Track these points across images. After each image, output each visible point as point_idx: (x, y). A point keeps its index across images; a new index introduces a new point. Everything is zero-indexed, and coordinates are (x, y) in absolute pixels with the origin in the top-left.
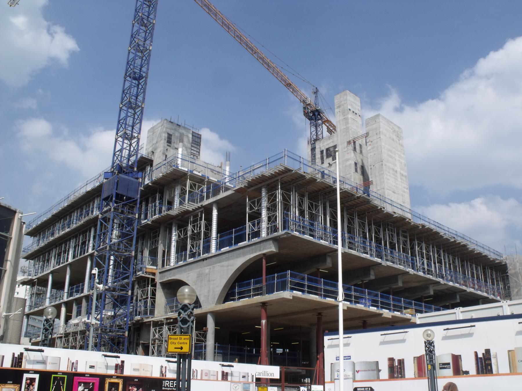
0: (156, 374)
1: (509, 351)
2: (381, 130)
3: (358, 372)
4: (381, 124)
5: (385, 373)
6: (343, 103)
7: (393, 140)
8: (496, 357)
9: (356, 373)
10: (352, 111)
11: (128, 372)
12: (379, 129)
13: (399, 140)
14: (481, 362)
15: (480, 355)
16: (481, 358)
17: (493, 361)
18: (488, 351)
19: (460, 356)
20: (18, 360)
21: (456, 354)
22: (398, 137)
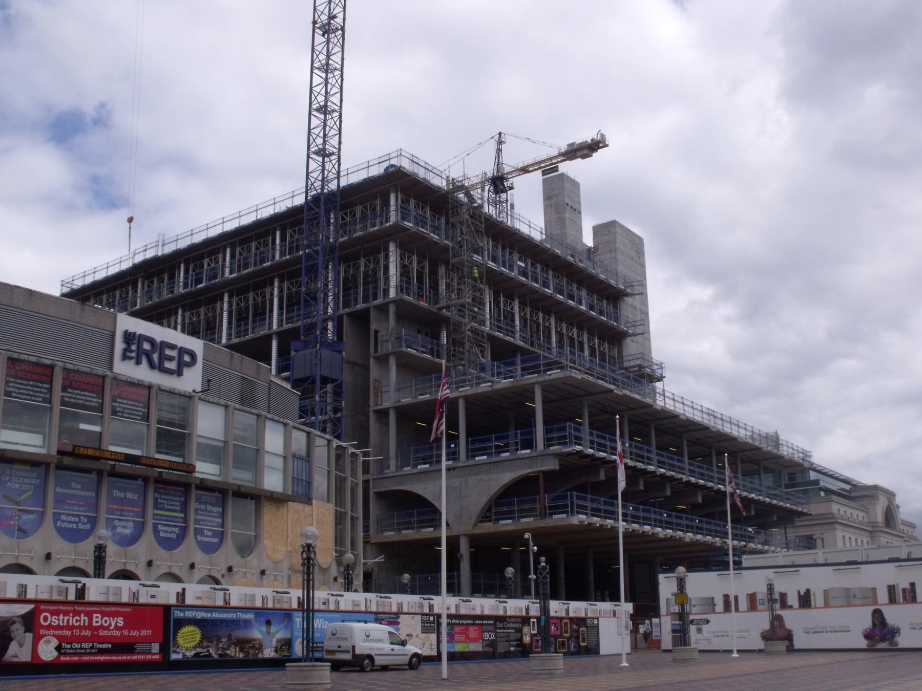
1: (825, 591)
2: (618, 245)
3: (694, 606)
4: (618, 236)
5: (720, 607)
6: (556, 192)
7: (632, 259)
8: (814, 595)
9: (692, 607)
10: (570, 206)
12: (615, 245)
13: (639, 258)
14: (803, 599)
15: (802, 593)
16: (802, 596)
17: (812, 598)
18: (808, 591)
19: (786, 594)
21: (783, 591)
22: (638, 252)
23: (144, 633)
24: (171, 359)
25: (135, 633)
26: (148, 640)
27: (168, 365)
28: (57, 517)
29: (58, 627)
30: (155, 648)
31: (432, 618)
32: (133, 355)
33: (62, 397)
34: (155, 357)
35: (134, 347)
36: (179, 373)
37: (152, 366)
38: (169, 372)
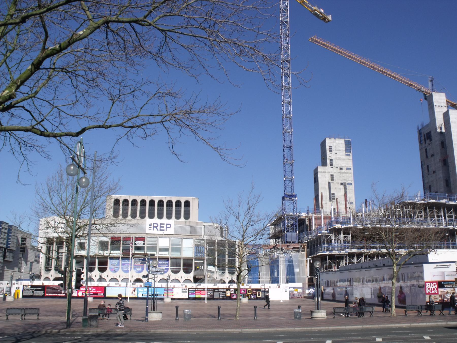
0: (259, 288)
11: (252, 288)
20: (229, 287)
23: (100, 291)
24: (163, 227)
25: (98, 292)
26: (101, 293)
27: (162, 229)
28: (122, 268)
29: (82, 290)
30: (102, 294)
31: (186, 289)
32: (152, 228)
33: (123, 243)
34: (158, 228)
35: (152, 227)
36: (166, 230)
37: (158, 230)
38: (164, 230)
